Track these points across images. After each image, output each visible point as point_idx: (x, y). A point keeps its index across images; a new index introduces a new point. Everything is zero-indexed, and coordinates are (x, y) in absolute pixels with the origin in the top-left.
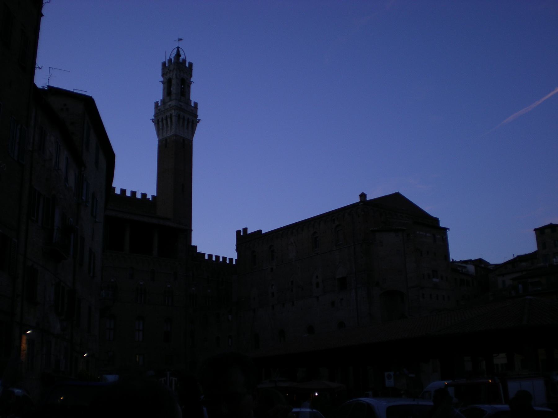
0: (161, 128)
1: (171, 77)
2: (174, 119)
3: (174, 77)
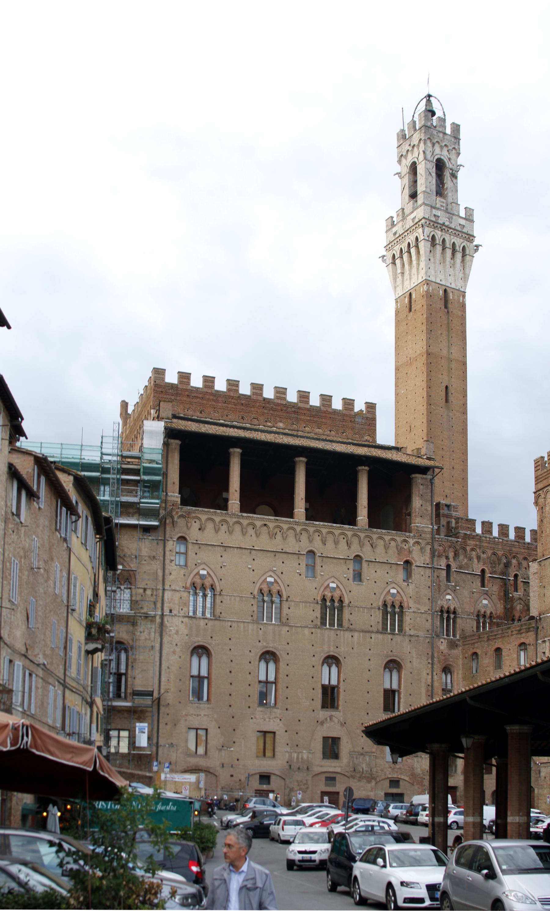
0: (399, 271)
1: (416, 160)
2: (421, 245)
3: (421, 157)
